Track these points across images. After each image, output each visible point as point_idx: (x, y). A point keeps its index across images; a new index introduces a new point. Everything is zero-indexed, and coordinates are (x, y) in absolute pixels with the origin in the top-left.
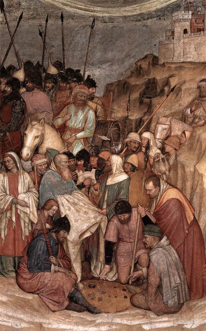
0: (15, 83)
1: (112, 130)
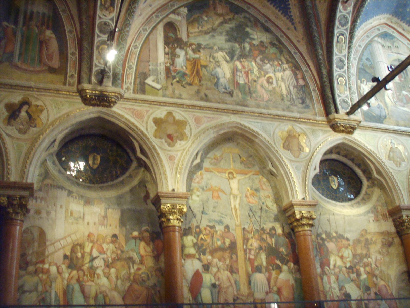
0: (322, 239)
1: (358, 257)
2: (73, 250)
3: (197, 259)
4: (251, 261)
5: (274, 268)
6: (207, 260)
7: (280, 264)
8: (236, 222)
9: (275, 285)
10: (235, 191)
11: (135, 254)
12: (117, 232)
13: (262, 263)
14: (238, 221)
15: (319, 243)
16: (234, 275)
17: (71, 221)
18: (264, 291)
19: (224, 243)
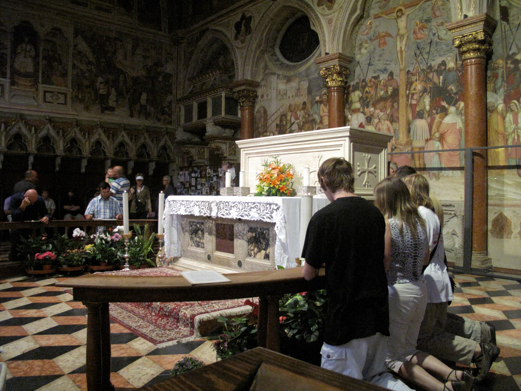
2: (281, 121)
3: (362, 112)
4: (413, 107)
5: (438, 112)
6: (370, 112)
7: (447, 106)
8: (401, 65)
9: (438, 131)
10: (402, 31)
11: (317, 116)
12: (305, 100)
13: (425, 108)
14: (402, 64)
15: (508, 68)
16: (394, 124)
17: (279, 98)
18: (424, 139)
19: (387, 92)
